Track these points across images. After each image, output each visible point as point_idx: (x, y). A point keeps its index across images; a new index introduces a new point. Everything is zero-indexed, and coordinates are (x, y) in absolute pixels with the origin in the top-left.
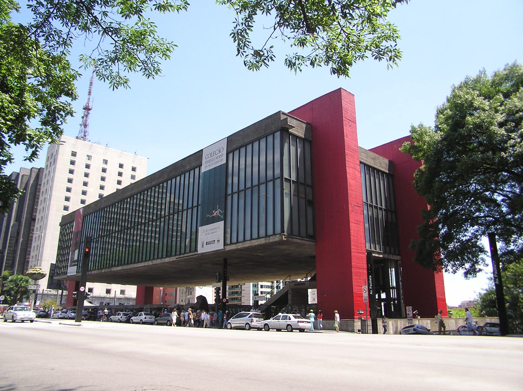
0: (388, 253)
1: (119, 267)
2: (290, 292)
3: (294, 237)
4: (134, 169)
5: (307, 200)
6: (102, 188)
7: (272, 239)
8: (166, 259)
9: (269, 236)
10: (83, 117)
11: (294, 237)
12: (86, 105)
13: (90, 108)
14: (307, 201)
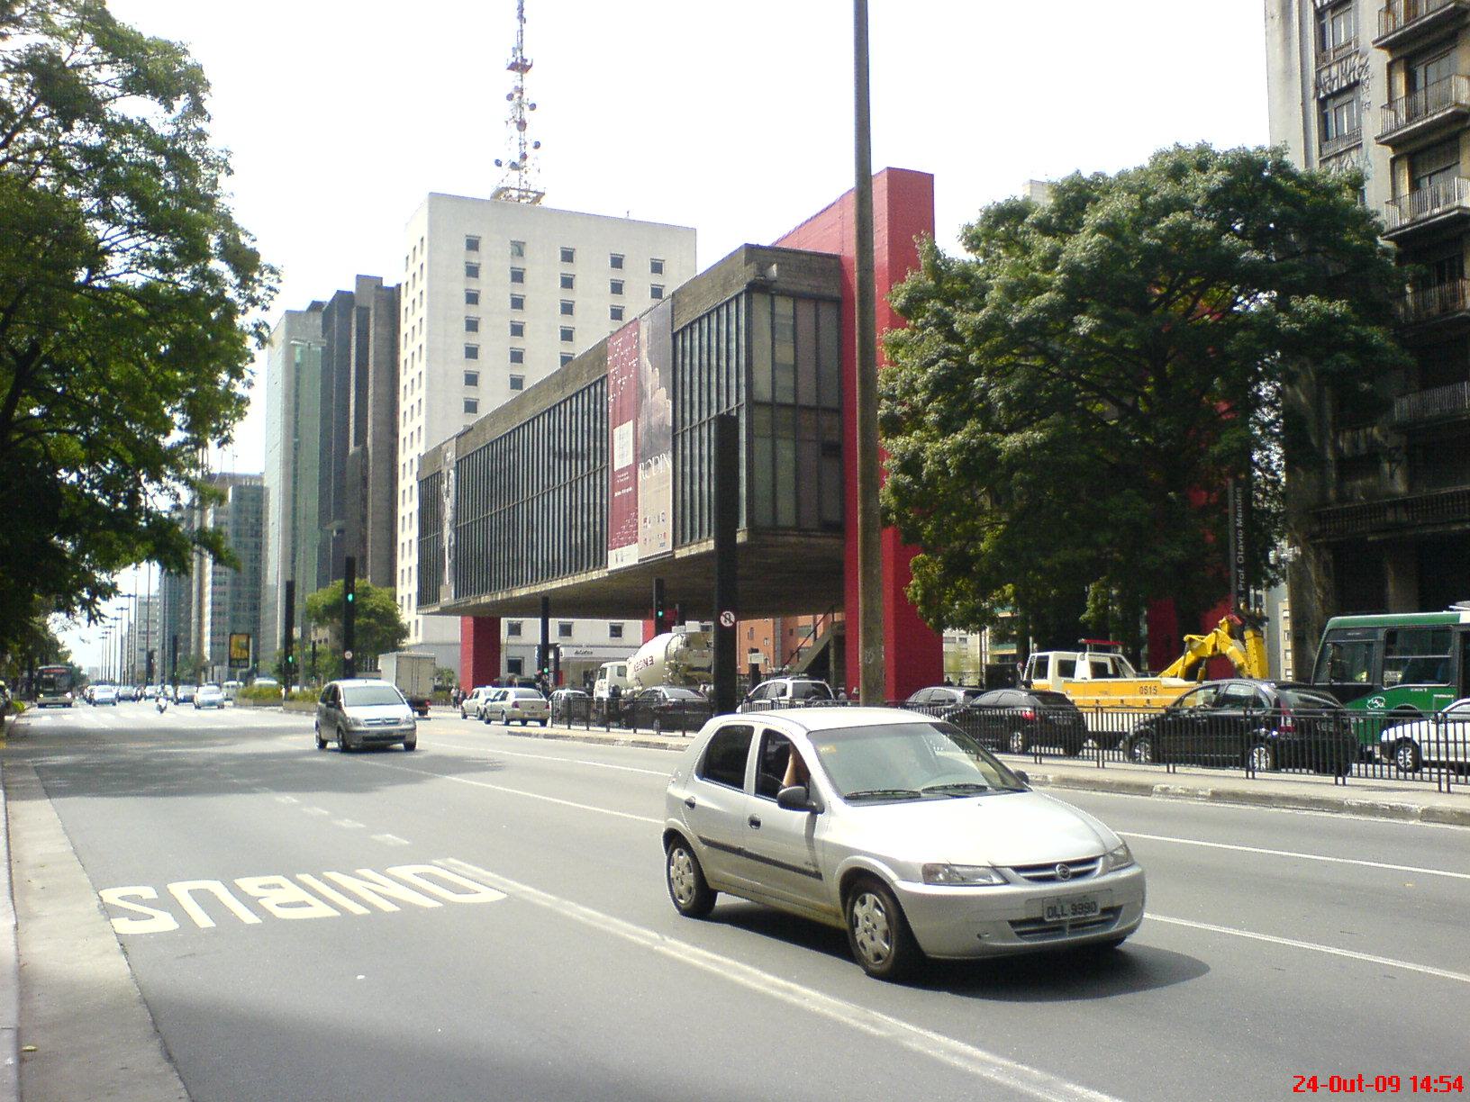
2: (832, 644)
4: (657, 268)
6: (567, 335)
10: (510, 97)
13: (528, 63)
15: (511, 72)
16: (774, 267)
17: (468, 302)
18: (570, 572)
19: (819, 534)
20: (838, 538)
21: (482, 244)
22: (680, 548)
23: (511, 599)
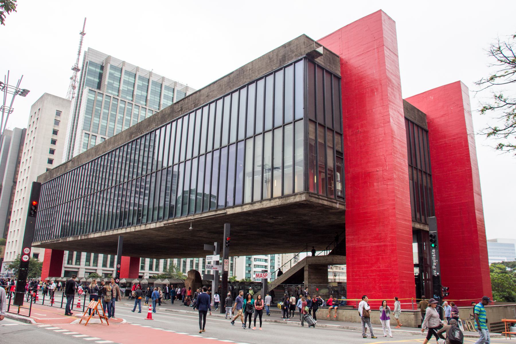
0: (423, 223)
1: (97, 234)
2: (306, 268)
5: (336, 151)
7: (292, 200)
8: (152, 225)
9: (289, 196)
10: (72, 78)
12: (75, 65)
14: (335, 152)
15: (73, 71)
17: (53, 134)
18: (83, 233)
21: (62, 115)
23: (88, 239)
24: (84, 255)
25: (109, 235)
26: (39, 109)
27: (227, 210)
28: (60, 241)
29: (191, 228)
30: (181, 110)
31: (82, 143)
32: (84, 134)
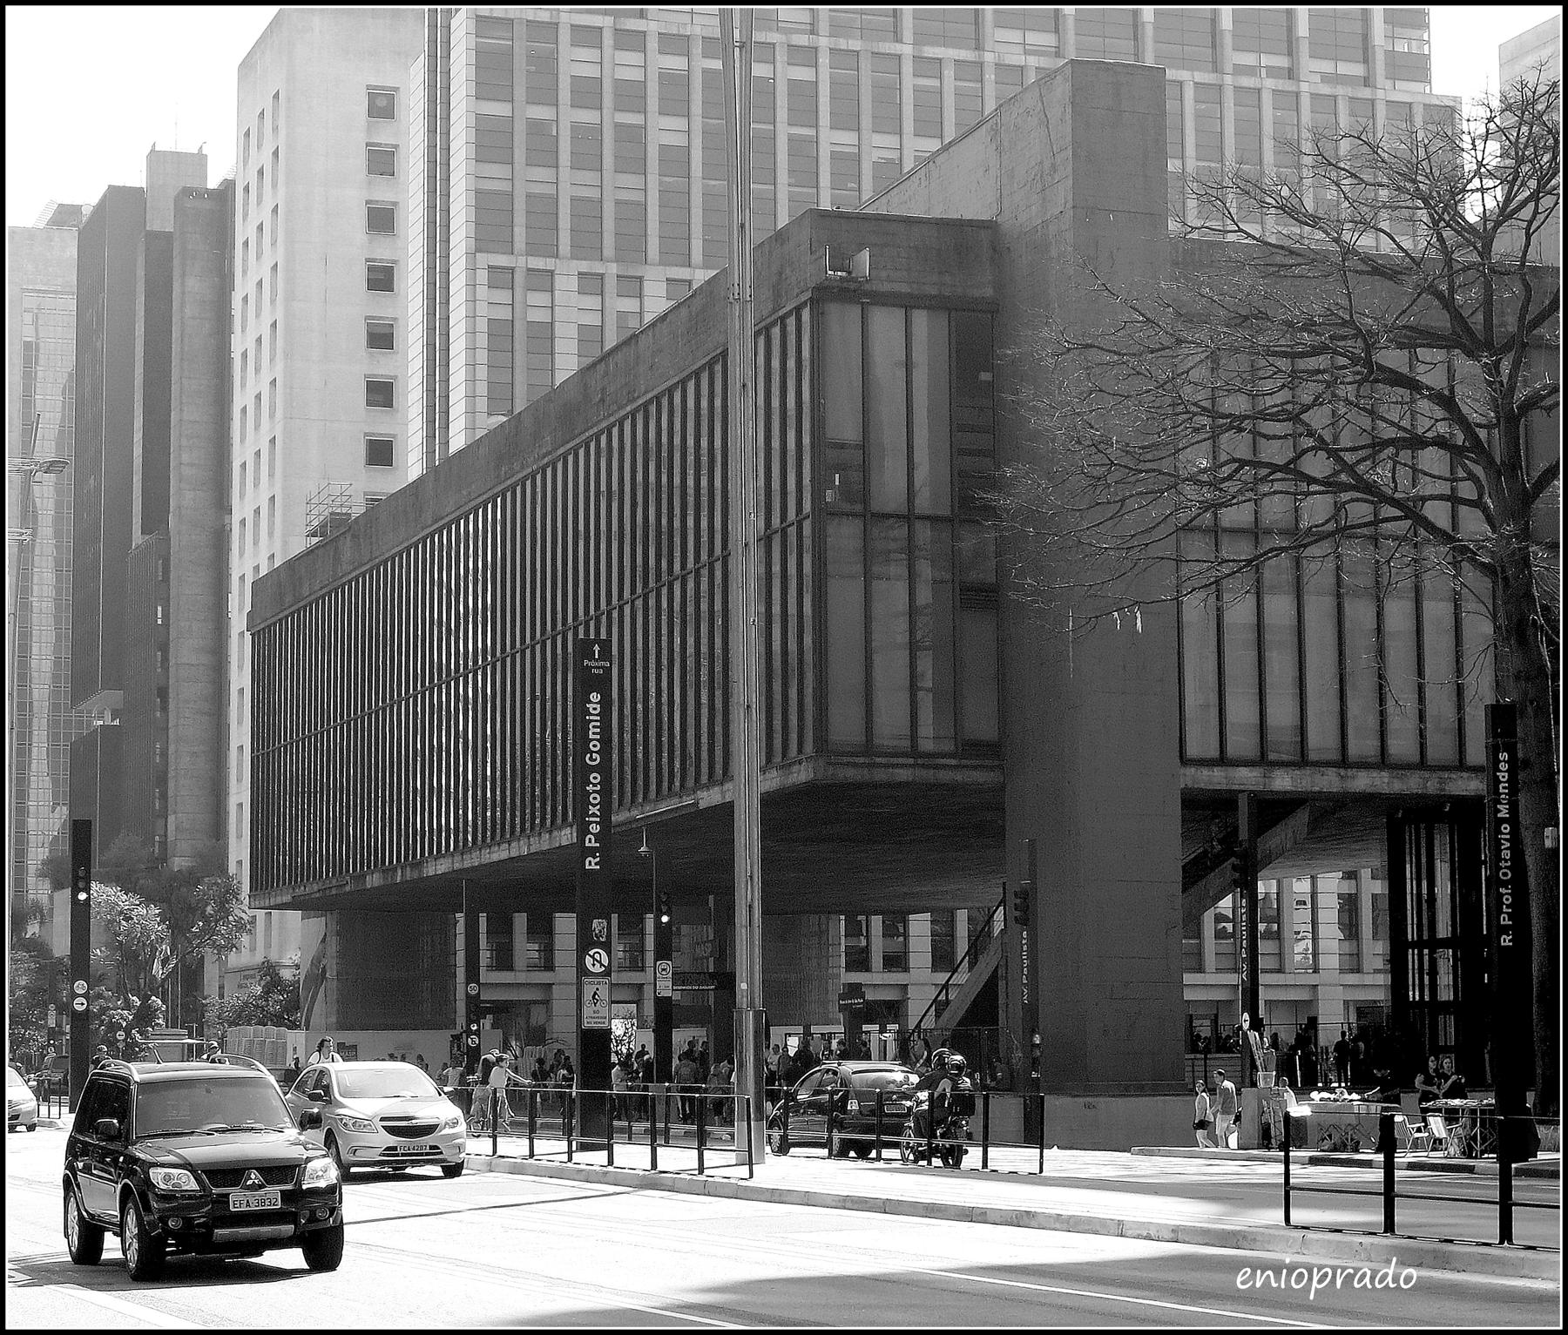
3: (878, 760)
11: (878, 760)
16: (865, 256)
19: (953, 762)
20: (992, 768)
22: (707, 787)
23: (422, 879)
24: (566, 924)
25: (481, 865)
26: (276, 96)
27: (702, 794)
28: (348, 888)
29: (642, 849)
30: (602, 400)
31: (482, 325)
32: (482, 276)
